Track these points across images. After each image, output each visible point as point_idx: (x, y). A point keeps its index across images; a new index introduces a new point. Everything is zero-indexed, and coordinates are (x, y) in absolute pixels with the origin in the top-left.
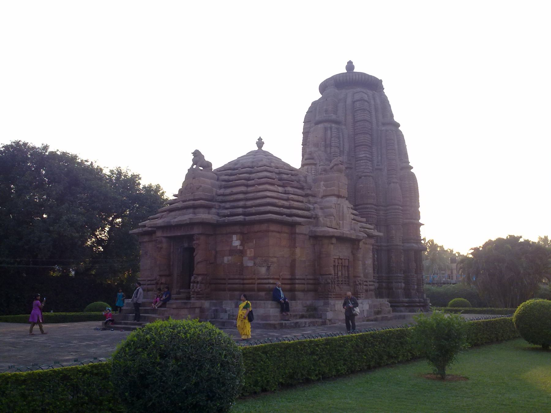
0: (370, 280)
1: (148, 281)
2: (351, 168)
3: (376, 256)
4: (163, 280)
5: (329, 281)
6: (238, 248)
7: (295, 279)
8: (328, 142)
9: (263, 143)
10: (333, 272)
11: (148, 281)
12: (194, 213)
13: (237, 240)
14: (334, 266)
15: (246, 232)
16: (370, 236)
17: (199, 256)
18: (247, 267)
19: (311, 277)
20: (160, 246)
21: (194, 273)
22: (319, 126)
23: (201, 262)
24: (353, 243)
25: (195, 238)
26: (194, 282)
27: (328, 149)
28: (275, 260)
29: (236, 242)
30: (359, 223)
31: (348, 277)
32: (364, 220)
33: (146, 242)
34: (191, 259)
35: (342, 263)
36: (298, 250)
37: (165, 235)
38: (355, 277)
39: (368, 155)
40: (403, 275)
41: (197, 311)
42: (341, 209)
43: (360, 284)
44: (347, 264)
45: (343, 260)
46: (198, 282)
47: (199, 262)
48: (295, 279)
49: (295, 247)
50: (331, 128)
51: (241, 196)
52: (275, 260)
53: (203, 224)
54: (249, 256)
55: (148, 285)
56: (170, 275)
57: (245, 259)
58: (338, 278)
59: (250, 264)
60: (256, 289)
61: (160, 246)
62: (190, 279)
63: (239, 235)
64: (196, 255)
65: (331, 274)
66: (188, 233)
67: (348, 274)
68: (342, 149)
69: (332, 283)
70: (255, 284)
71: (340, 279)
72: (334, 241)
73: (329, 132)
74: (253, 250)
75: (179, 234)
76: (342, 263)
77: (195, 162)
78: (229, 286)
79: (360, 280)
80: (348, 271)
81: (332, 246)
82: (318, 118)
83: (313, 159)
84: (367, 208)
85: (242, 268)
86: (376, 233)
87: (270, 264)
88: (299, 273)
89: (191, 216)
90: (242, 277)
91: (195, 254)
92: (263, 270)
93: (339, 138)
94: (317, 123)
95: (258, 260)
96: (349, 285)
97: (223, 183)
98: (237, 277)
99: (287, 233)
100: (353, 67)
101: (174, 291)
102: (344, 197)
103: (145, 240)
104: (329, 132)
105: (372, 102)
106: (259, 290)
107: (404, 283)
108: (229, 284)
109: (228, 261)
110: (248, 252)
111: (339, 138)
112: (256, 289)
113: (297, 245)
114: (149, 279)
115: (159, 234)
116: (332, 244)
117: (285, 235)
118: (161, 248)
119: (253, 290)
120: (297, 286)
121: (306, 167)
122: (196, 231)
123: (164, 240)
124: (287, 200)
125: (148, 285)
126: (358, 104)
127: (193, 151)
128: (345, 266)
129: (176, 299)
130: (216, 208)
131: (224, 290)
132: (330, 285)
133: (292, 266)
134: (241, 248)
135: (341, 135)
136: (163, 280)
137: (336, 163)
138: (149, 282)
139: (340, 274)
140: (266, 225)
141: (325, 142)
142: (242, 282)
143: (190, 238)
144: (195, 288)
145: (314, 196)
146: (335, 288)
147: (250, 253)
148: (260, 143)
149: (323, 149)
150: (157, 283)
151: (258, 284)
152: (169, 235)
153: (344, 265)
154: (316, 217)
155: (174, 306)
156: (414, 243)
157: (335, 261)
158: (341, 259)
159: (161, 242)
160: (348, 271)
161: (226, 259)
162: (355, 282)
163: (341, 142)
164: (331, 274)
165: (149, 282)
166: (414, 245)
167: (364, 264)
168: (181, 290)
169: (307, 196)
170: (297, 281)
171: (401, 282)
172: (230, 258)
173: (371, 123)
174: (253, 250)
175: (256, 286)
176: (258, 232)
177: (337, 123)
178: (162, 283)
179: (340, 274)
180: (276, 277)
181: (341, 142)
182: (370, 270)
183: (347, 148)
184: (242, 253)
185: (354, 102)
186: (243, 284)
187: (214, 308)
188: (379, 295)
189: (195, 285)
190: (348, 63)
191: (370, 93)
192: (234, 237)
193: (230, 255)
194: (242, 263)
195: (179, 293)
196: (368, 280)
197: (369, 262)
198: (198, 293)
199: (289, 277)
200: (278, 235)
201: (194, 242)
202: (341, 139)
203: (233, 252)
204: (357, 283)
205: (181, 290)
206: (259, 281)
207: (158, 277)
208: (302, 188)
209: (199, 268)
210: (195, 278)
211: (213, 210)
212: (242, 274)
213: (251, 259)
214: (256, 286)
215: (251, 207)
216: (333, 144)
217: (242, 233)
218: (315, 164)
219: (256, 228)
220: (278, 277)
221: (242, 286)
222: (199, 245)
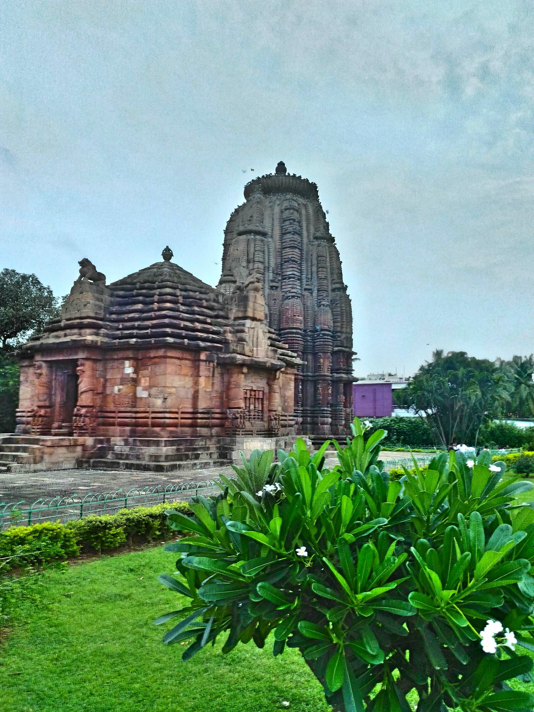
0: (291, 414)
2: (277, 287)
3: (301, 387)
4: (42, 412)
5: (238, 416)
7: (198, 413)
8: (251, 256)
9: (172, 255)
10: (242, 405)
12: (80, 335)
13: (129, 367)
14: (246, 398)
15: (140, 358)
16: (291, 365)
17: (84, 384)
18: (141, 398)
19: (218, 411)
20: (39, 371)
21: (78, 404)
22: (241, 237)
23: (85, 392)
24: (269, 372)
25: (79, 363)
26: (76, 415)
27: (251, 266)
28: (173, 390)
29: (129, 370)
30: (279, 350)
31: (262, 411)
32: (287, 346)
33: (26, 366)
34: (77, 386)
35: (255, 395)
36: (202, 380)
37: (45, 359)
38: (270, 411)
39: (295, 273)
40: (329, 409)
41: (79, 449)
42: (255, 334)
43: (275, 419)
44: (261, 397)
45: (257, 392)
46: (81, 416)
47: (82, 393)
48: (198, 413)
49: (198, 376)
50: (255, 240)
51: (136, 315)
52: (173, 390)
53: (91, 347)
56: (51, 406)
57: (139, 389)
58: (249, 412)
59: (145, 394)
61: (39, 371)
62: (73, 411)
63: (132, 361)
64: (80, 383)
65: (240, 408)
66: (71, 358)
67: (263, 407)
68: (267, 265)
69: (241, 418)
70: (148, 418)
71: (252, 414)
72: (245, 370)
73: (252, 245)
74: (148, 378)
75: (61, 358)
76: (255, 395)
77: (83, 274)
78: (119, 419)
79: (276, 415)
80: (262, 404)
81: (243, 376)
82: (241, 229)
83: (232, 276)
84: (293, 333)
85: (135, 399)
86: (298, 361)
87: (166, 395)
88: (202, 405)
89: (74, 338)
90: (134, 409)
91: (79, 381)
92: (159, 402)
93: (263, 252)
94: (240, 234)
95: (154, 391)
96: (262, 419)
97: (118, 299)
98: (129, 409)
99: (189, 360)
100: (285, 170)
101: (56, 425)
102: (259, 320)
104: (252, 245)
105: (304, 212)
106: (154, 425)
107: (331, 418)
108: (119, 418)
109: (119, 390)
110: (143, 381)
111: (263, 252)
112: (150, 423)
113: (201, 373)
114: (29, 410)
115: (38, 358)
116: (243, 373)
117: (187, 362)
118: (41, 374)
119: (146, 425)
120: (199, 421)
121: (224, 285)
122: (81, 355)
123: (44, 365)
124: (192, 321)
126: (286, 214)
127: (80, 260)
128: (258, 399)
129: (56, 435)
130: (107, 329)
131: (113, 424)
132: (239, 420)
133: (195, 397)
134: (134, 376)
135: (266, 249)
136: (42, 412)
137: (252, 280)
139: (252, 407)
140: (163, 350)
141: (248, 256)
142: (134, 415)
143: (74, 363)
145: (226, 318)
146: (244, 422)
147: (144, 382)
148: (167, 254)
149: (244, 264)
150: (34, 416)
151: (153, 418)
152: (49, 359)
153: (257, 397)
154: (226, 342)
155: (49, 444)
156: (343, 373)
157: (246, 393)
158: (255, 391)
159: (40, 367)
160: (262, 404)
161: (116, 388)
162: (270, 416)
163: (266, 258)
164: (240, 408)
166: (344, 376)
167: (284, 398)
168: (63, 424)
169: (217, 317)
170: (200, 416)
171: (327, 417)
172: (121, 387)
173: (300, 234)
174: (148, 378)
175: (150, 421)
177: (264, 234)
178: (40, 416)
179: (252, 407)
180: (173, 410)
181: (266, 258)
182: (292, 403)
183: (272, 264)
184: (135, 382)
185: (282, 212)
187: (99, 446)
188: (302, 431)
190: (279, 164)
191: (301, 200)
192: (127, 363)
193: (121, 385)
194: (135, 393)
195: (60, 427)
196: (286, 414)
197: (290, 393)
198: (81, 428)
199: (191, 410)
200: (177, 362)
201: (78, 368)
202: (266, 253)
203: (124, 381)
204: (272, 417)
205: (63, 424)
206: (154, 415)
207: (36, 408)
208: (211, 308)
209: (85, 399)
210: (78, 410)
211: (103, 331)
212: (135, 407)
213: (145, 389)
214: (150, 421)
215: (147, 328)
216: (256, 259)
217: (135, 359)
218: (235, 282)
219: (152, 354)
220: (176, 410)
221: (134, 420)
222: (84, 372)
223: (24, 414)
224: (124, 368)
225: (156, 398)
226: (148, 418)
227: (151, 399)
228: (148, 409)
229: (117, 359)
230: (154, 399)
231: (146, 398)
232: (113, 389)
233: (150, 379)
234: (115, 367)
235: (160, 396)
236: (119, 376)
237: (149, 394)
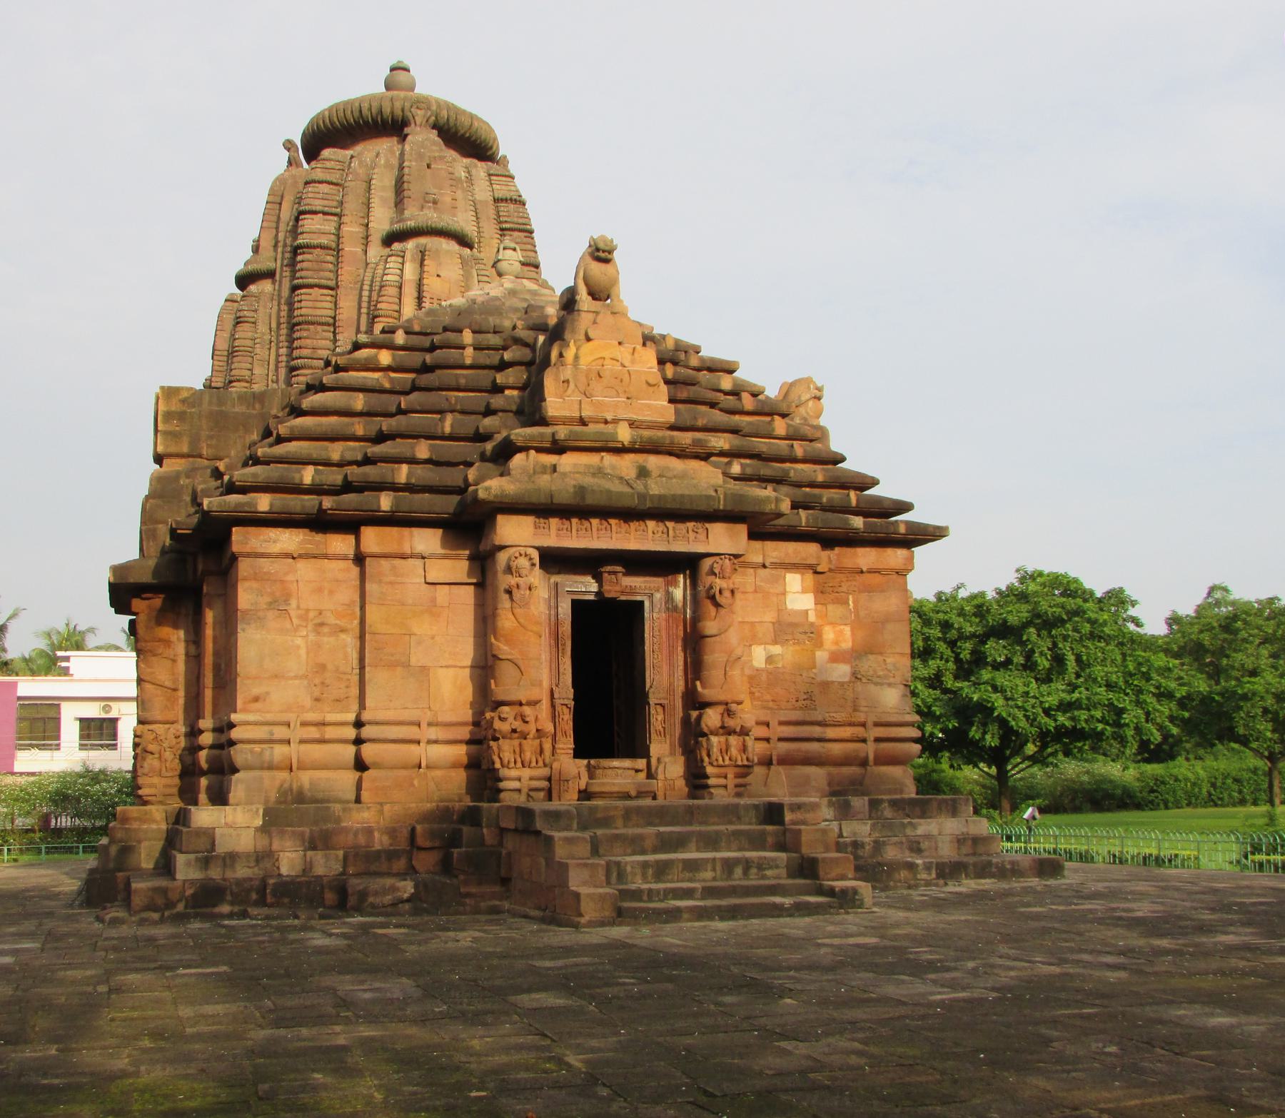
1: (304, 724)
6: (812, 617)
11: (304, 724)
13: (804, 591)
29: (798, 595)
46: (744, 732)
54: (834, 648)
55: (302, 741)
60: (871, 757)
63: (809, 576)
70: (864, 741)
103: (276, 548)
109: (770, 659)
112: (871, 757)
114: (312, 716)
125: (302, 741)
138: (313, 733)
144: (734, 751)
151: (877, 740)
165: (313, 733)
172: (776, 649)
176: (869, 572)
186: (819, 740)
189: (733, 740)
192: (794, 581)
193: (775, 642)
203: (786, 629)
214: (870, 749)
223: (280, 732)
224: (784, 593)
225: (876, 684)
226: (864, 741)
227: (859, 687)
228: (861, 717)
229: (764, 566)
230: (872, 687)
231: (842, 684)
232: (750, 654)
233: (852, 630)
234: (750, 589)
235: (892, 680)
236: (769, 617)
237: (856, 676)
